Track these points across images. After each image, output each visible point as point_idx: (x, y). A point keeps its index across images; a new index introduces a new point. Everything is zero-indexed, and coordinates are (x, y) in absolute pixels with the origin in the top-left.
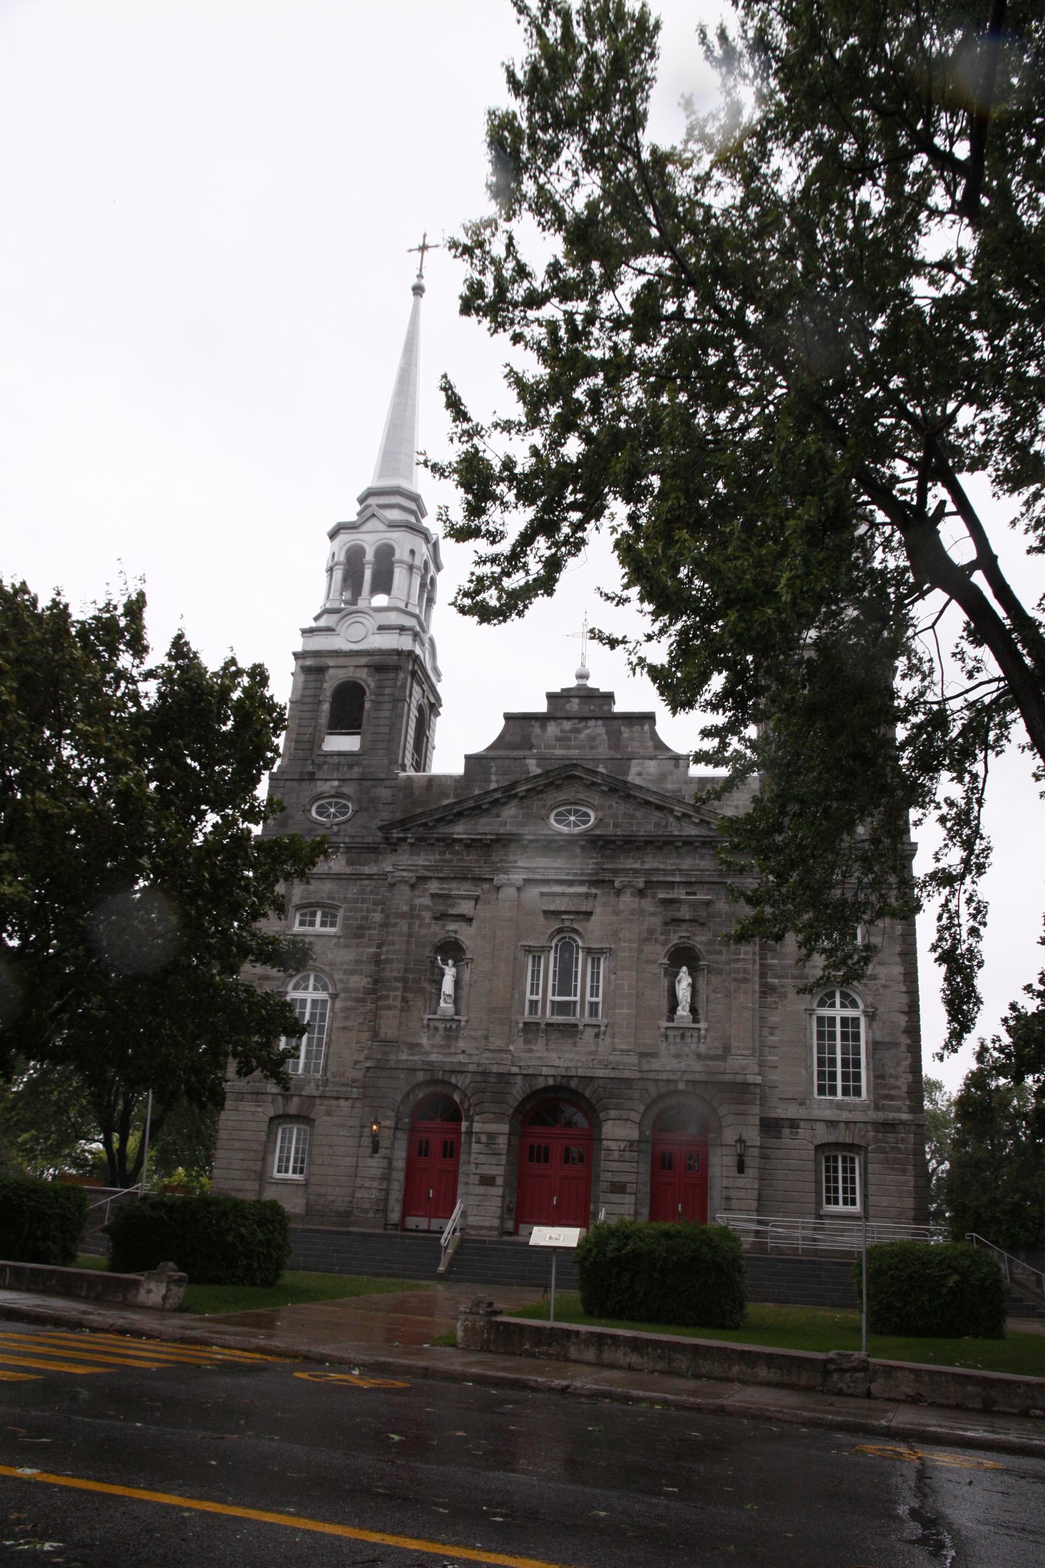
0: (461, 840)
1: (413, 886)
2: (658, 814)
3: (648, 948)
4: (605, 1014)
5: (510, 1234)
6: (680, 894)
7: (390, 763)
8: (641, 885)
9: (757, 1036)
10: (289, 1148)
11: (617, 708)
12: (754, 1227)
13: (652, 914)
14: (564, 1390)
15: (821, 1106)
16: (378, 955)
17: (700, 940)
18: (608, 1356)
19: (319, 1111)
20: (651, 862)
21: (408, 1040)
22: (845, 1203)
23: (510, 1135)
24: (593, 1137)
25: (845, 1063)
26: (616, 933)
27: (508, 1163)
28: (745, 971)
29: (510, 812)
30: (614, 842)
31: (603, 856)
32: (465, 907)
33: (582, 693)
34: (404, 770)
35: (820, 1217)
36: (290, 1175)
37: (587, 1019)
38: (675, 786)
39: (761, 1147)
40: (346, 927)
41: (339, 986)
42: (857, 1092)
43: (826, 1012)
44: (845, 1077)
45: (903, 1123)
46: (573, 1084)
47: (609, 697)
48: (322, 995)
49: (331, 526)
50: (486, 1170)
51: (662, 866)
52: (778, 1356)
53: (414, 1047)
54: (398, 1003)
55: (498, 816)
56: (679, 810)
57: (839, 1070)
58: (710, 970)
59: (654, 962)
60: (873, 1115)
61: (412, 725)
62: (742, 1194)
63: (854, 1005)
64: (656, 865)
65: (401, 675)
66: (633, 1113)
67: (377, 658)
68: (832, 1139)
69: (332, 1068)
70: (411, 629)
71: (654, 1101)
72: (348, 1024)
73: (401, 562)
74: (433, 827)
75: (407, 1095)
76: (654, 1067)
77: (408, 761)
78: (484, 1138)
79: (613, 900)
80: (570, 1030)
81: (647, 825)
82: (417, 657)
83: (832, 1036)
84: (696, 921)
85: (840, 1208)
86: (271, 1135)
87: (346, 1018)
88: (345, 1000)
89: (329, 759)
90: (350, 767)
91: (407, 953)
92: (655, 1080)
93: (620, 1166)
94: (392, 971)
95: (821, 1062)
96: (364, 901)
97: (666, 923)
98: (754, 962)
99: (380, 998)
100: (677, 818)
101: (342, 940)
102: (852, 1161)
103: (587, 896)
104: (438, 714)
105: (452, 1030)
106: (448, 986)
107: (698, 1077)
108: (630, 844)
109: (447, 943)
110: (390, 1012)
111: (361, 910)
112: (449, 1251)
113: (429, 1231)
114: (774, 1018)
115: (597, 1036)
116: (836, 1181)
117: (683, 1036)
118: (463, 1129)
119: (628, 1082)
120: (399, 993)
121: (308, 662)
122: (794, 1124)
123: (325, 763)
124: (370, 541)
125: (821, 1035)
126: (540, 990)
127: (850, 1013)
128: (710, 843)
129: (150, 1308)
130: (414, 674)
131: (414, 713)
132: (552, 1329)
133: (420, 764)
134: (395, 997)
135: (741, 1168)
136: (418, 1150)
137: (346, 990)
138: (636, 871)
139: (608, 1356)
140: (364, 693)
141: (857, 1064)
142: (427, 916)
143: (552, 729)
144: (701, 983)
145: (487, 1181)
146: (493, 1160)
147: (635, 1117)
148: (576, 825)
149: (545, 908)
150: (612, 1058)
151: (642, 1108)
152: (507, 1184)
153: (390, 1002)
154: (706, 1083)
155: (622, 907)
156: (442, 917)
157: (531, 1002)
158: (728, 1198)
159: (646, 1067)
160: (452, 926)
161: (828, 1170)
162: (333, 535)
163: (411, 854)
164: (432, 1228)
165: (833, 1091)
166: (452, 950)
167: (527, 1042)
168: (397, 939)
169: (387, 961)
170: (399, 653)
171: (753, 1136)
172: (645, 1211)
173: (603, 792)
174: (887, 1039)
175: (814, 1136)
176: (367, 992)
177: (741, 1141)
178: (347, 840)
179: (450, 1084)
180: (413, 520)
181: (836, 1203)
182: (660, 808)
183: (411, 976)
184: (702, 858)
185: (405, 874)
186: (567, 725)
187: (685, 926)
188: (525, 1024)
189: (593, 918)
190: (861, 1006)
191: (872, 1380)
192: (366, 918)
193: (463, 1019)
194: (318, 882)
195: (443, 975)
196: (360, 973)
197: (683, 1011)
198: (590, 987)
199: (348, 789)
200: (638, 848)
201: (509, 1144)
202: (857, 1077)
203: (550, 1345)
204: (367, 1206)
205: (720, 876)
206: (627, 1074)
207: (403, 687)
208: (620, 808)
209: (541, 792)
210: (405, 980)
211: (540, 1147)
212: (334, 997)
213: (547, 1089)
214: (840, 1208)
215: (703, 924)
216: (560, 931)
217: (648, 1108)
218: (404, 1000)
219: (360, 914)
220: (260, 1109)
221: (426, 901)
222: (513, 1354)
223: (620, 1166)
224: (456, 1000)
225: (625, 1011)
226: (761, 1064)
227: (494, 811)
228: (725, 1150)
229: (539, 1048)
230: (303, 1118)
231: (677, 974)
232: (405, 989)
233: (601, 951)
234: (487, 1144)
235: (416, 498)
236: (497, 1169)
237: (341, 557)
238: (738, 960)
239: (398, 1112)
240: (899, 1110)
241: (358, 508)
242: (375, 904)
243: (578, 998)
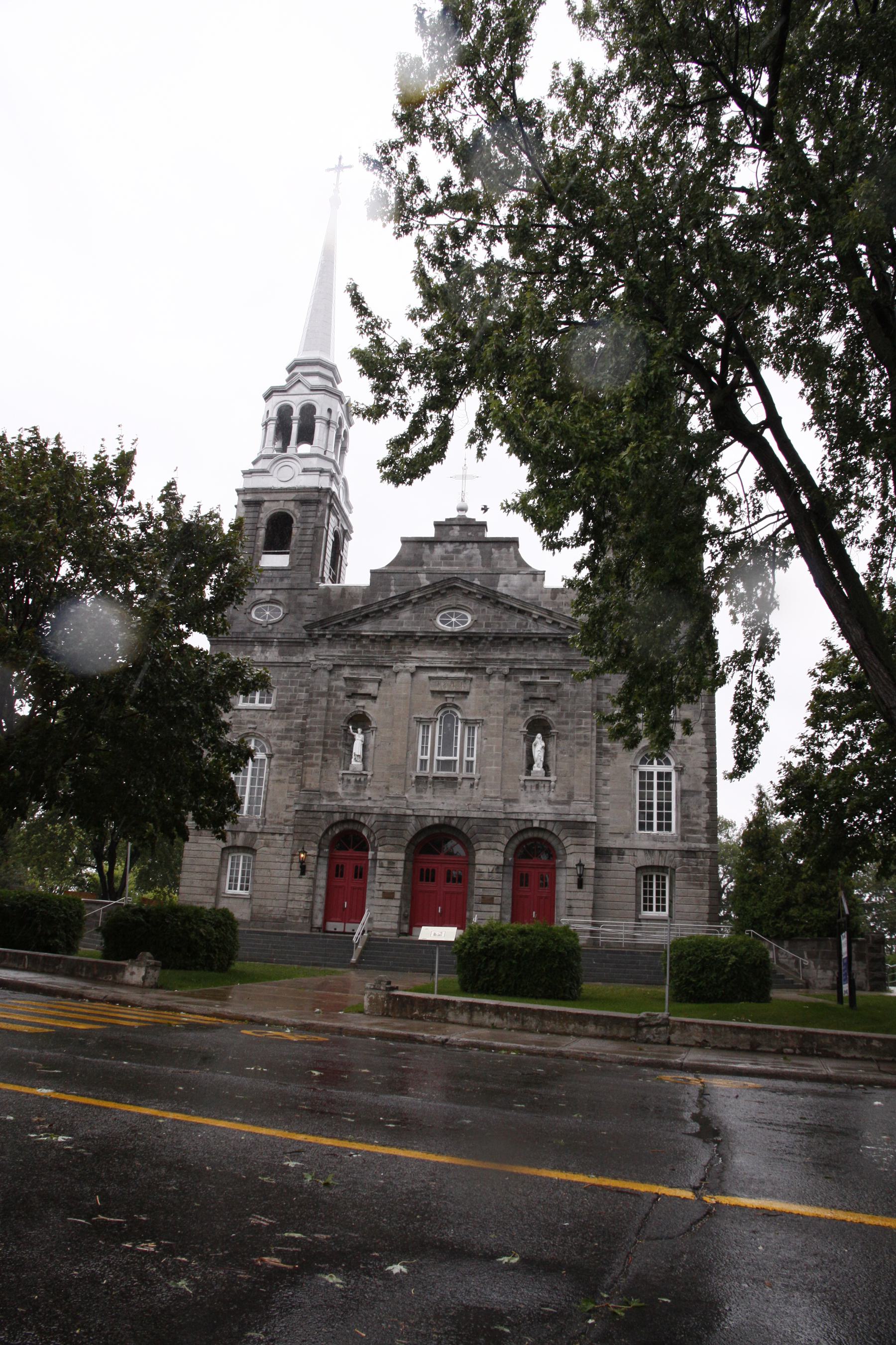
1: (330, 672)
2: (521, 617)
3: (512, 720)
4: (479, 770)
5: (406, 934)
6: (536, 678)
7: (312, 576)
8: (506, 671)
9: (594, 787)
10: (237, 871)
11: (489, 534)
12: (589, 928)
14: (444, 1043)
15: (642, 839)
16: (303, 724)
17: (551, 713)
18: (476, 1019)
19: (259, 844)
20: (514, 654)
21: (327, 790)
22: (658, 910)
23: (405, 861)
24: (468, 863)
25: (660, 807)
26: (486, 708)
27: (404, 882)
28: (585, 736)
29: (406, 615)
32: (371, 688)
33: (462, 522)
34: (323, 582)
35: (639, 920)
36: (238, 891)
37: (464, 774)
38: (534, 595)
39: (596, 869)
40: (278, 703)
41: (274, 749)
42: (669, 827)
43: (646, 768)
44: (660, 816)
45: (702, 851)
46: (454, 823)
47: (483, 526)
49: (265, 389)
50: (386, 887)
51: (522, 657)
52: (603, 1016)
53: (332, 795)
54: (319, 761)
55: (396, 618)
56: (536, 613)
57: (655, 811)
58: (559, 736)
59: (516, 730)
60: (680, 845)
61: (330, 547)
62: (581, 904)
63: (668, 762)
64: (518, 656)
65: (321, 508)
67: (302, 495)
68: (649, 863)
69: (269, 811)
70: (329, 471)
71: (515, 835)
72: (282, 777)
73: (321, 418)
74: (346, 626)
75: (326, 832)
76: (516, 810)
77: (326, 575)
78: (385, 864)
79: (485, 683)
80: (452, 782)
81: (513, 624)
82: (334, 493)
83: (651, 786)
84: (548, 699)
85: (654, 913)
86: (223, 861)
87: (280, 773)
88: (279, 759)
89: (264, 573)
90: (282, 579)
91: (326, 723)
93: (489, 884)
94: (314, 737)
95: (642, 806)
96: (292, 683)
97: (525, 701)
98: (592, 730)
99: (305, 758)
100: (535, 620)
102: (664, 879)
103: (465, 679)
104: (349, 539)
105: (361, 782)
106: (357, 748)
107: (548, 817)
109: (356, 716)
110: (313, 769)
111: (290, 690)
112: (360, 947)
113: (344, 933)
114: (606, 773)
115: (472, 786)
116: (651, 893)
117: (537, 787)
118: (370, 857)
119: (495, 821)
120: (320, 754)
121: (248, 497)
122: (620, 852)
123: (261, 576)
124: (296, 402)
125: (642, 786)
126: (428, 751)
127: (664, 769)
128: (560, 639)
129: (133, 985)
130: (331, 506)
131: (331, 538)
132: (435, 1000)
133: (334, 579)
134: (317, 757)
135: (580, 884)
136: (335, 872)
137: (280, 752)
138: (503, 660)
139: (476, 1019)
140: (292, 521)
141: (669, 807)
142: (342, 695)
143: (439, 550)
144: (552, 746)
145: (388, 895)
146: (393, 879)
147: (502, 847)
148: (456, 625)
150: (483, 803)
151: (506, 840)
152: (403, 898)
153: (314, 761)
154: (555, 821)
155: (492, 689)
156: (353, 695)
157: (422, 761)
158: (570, 907)
159: (509, 810)
160: (361, 703)
161: (645, 886)
162: (267, 397)
163: (329, 647)
164: (347, 930)
165: (650, 827)
166: (360, 721)
167: (418, 791)
168: (318, 712)
169: (311, 729)
170: (319, 490)
171: (590, 861)
172: (508, 917)
174: (692, 788)
175: (635, 861)
176: (296, 753)
177: (580, 865)
178: (279, 636)
179: (360, 823)
180: (330, 385)
181: (651, 910)
182: (521, 612)
183: (329, 741)
184: (554, 650)
185: (324, 662)
186: (450, 547)
187: (539, 703)
189: (469, 697)
190: (673, 764)
191: (671, 1032)
193: (370, 773)
195: (354, 740)
196: (290, 738)
197: (538, 768)
198: (468, 748)
199: (279, 597)
200: (505, 643)
201: (405, 868)
202: (669, 817)
203: (433, 1011)
204: (297, 914)
205: (566, 664)
206: (494, 815)
207: (323, 517)
208: (491, 612)
209: (429, 599)
210: (324, 744)
211: (428, 870)
212: (270, 757)
213: (435, 826)
214: (654, 913)
215: (553, 702)
216: (444, 706)
217: (511, 840)
218: (324, 759)
221: (341, 683)
222: (407, 1018)
223: (489, 884)
224: (364, 760)
225: (494, 767)
226: (596, 807)
227: (393, 614)
228: (569, 872)
229: (428, 795)
230: (248, 849)
231: (534, 739)
232: (324, 751)
233: (476, 722)
234: (388, 868)
235: (333, 368)
236: (396, 887)
237: (274, 414)
238: (580, 729)
239: (320, 844)
240: (699, 841)
241: (287, 375)
242: (302, 685)
243: (457, 758)
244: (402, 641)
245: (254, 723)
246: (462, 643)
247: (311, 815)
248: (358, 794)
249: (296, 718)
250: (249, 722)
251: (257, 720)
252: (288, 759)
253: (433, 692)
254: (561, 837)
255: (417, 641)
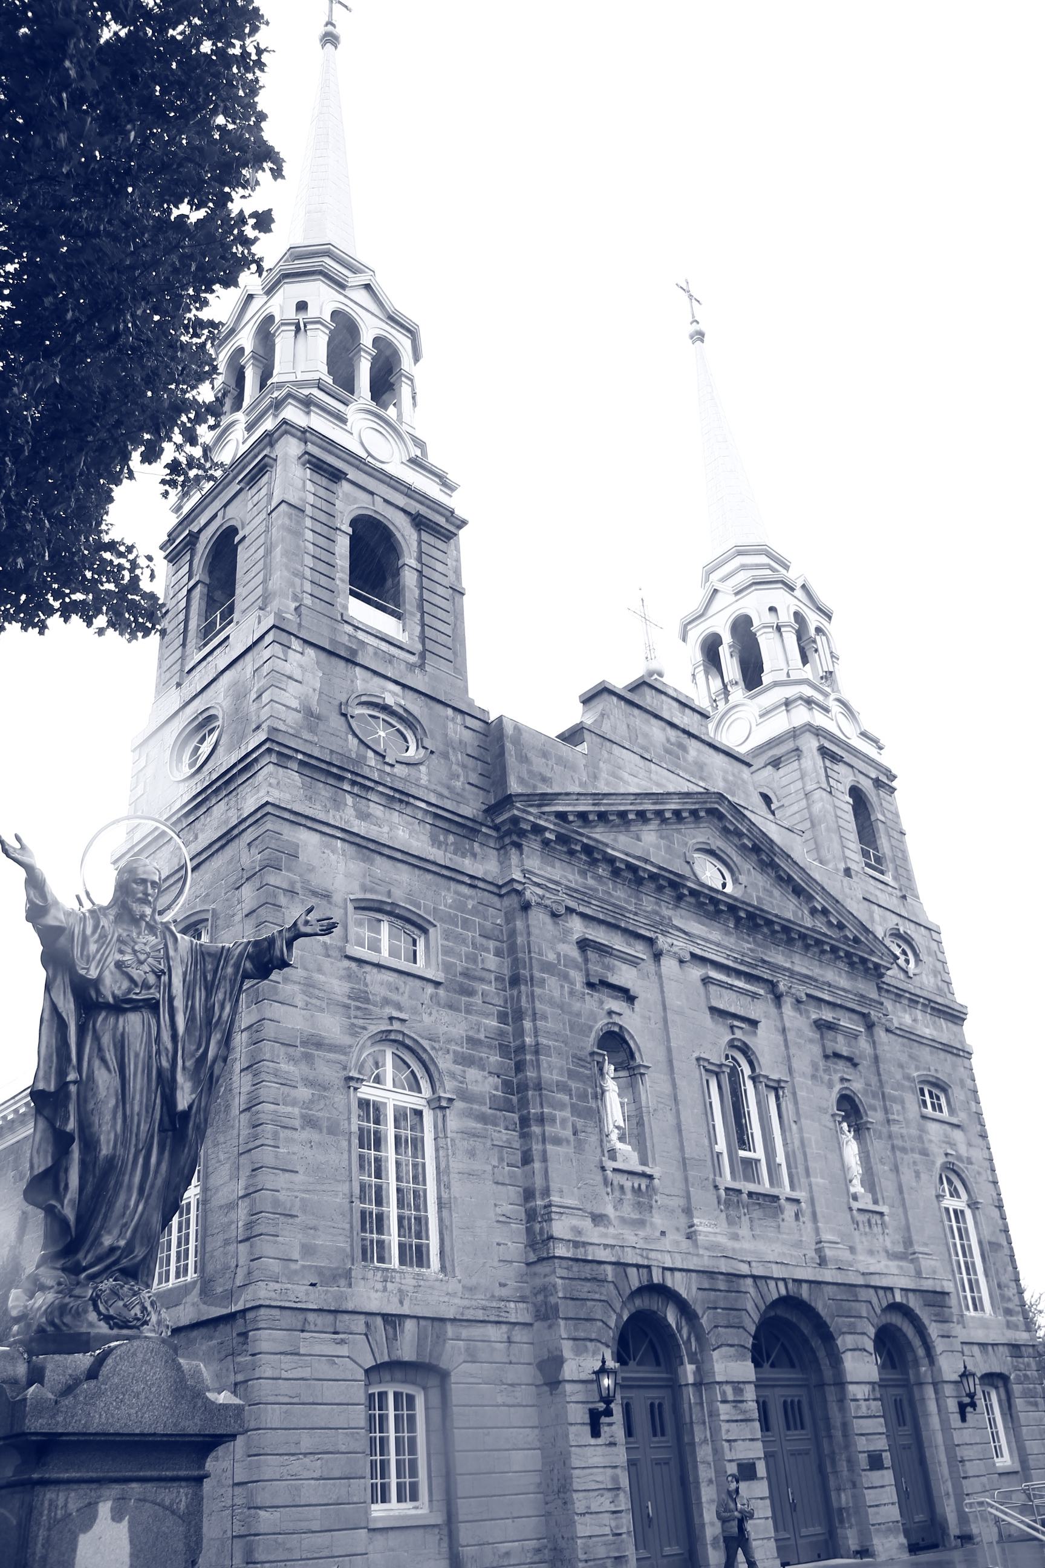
0: (611, 860)
13: (811, 1041)
30: (769, 923)
31: (755, 941)
32: (624, 976)
46: (805, 1292)
48: (412, 1101)
54: (568, 1133)
66: (865, 1337)
72: (477, 1166)
84: (849, 1059)
87: (472, 1154)
92: (876, 1288)
101: (441, 991)
108: (787, 935)
137: (464, 1095)
142: (578, 978)
145: (747, 1471)
149: (715, 1003)
156: (599, 985)
167: (730, 1222)
173: (744, 846)
182: (798, 891)
188: (727, 1189)
192: (472, 958)
194: (387, 864)
215: (855, 1065)
219: (464, 949)
220: (344, 1350)
229: (744, 1231)
244: (660, 889)
245: (399, 1007)
246: (738, 920)
247: (587, 1271)
248: (641, 1223)
249: (487, 1015)
250: (386, 1002)
251: (404, 1000)
252: (483, 1118)
253: (713, 1010)
254: (926, 1322)
255: (680, 898)
